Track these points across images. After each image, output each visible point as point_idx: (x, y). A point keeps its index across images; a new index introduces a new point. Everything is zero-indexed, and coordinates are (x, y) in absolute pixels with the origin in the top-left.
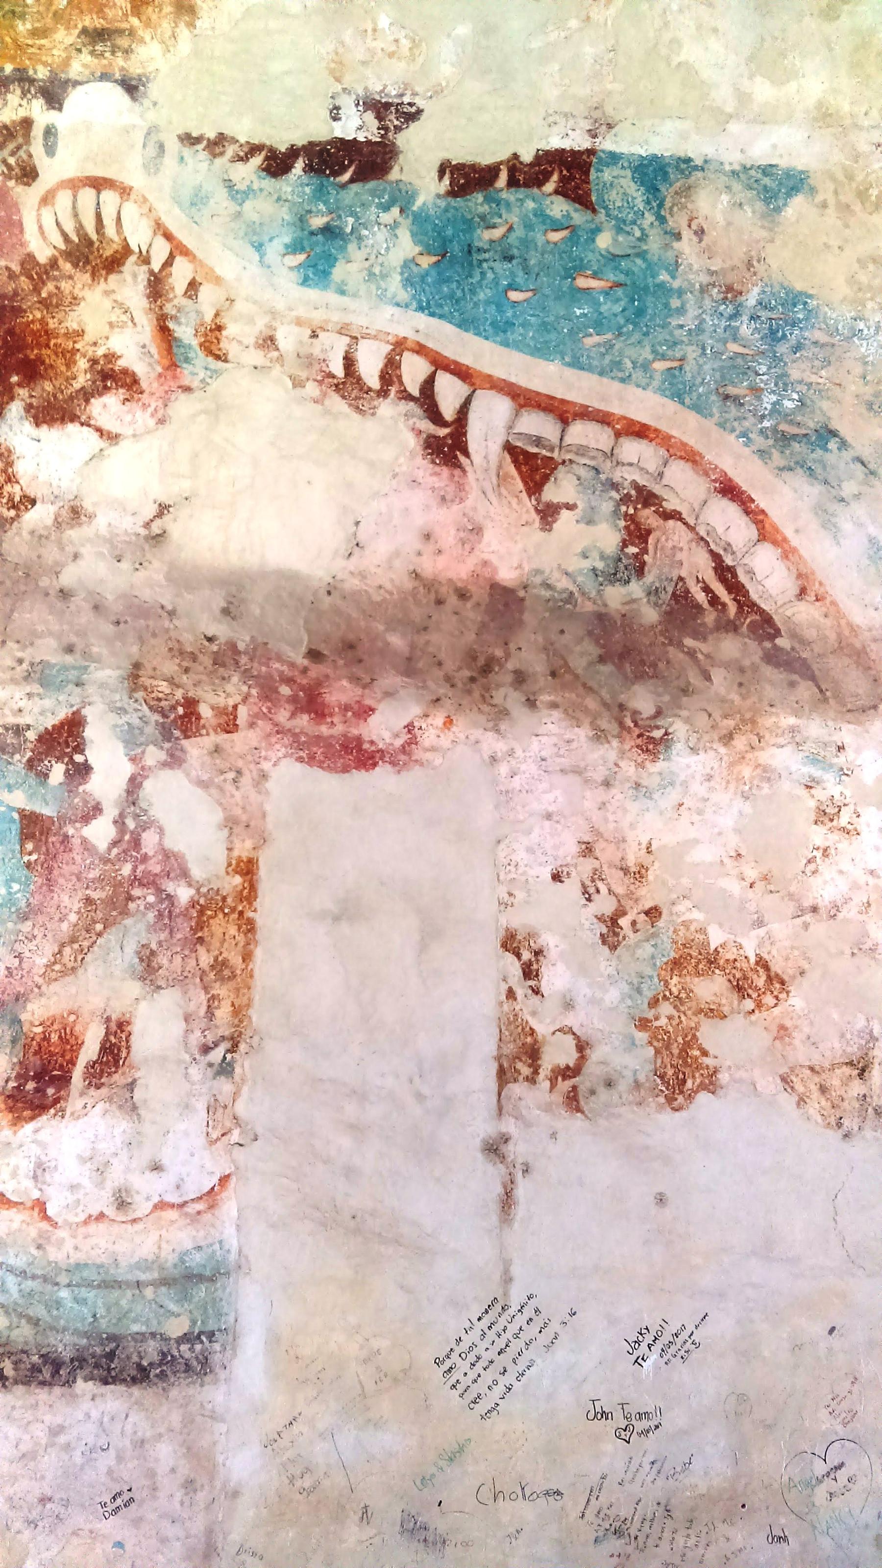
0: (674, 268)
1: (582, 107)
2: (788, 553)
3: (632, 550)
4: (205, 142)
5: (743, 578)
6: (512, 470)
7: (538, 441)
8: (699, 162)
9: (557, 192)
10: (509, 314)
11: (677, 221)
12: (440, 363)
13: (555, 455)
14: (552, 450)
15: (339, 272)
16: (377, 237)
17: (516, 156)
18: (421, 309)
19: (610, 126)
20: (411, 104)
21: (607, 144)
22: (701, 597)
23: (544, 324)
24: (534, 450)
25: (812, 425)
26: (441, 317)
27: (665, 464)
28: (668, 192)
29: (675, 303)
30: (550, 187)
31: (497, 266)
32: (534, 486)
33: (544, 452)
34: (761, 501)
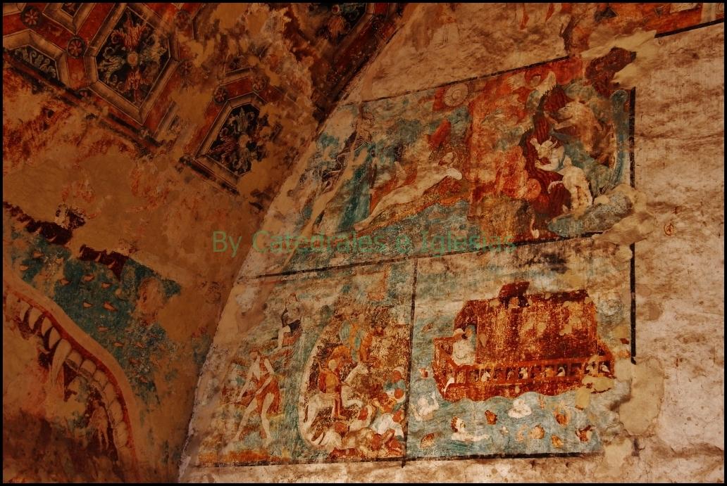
0: (133, 309)
1: (131, 240)
2: (128, 428)
3: (87, 415)
4: (11, 209)
5: (114, 434)
6: (62, 373)
7: (74, 364)
8: (155, 273)
9: (111, 269)
10: (82, 311)
11: (141, 292)
12: (56, 325)
13: (77, 371)
14: (76, 369)
15: (35, 279)
16: (53, 267)
17: (105, 251)
18: (56, 301)
19: (136, 250)
20: (82, 219)
21: (133, 257)
22: (100, 438)
23: (90, 319)
24: (71, 368)
25: (149, 380)
26: (61, 306)
27: (106, 384)
28: (142, 280)
29: (129, 322)
30: (110, 266)
31: (84, 291)
32: (67, 383)
33: (74, 369)
34: (128, 405)
